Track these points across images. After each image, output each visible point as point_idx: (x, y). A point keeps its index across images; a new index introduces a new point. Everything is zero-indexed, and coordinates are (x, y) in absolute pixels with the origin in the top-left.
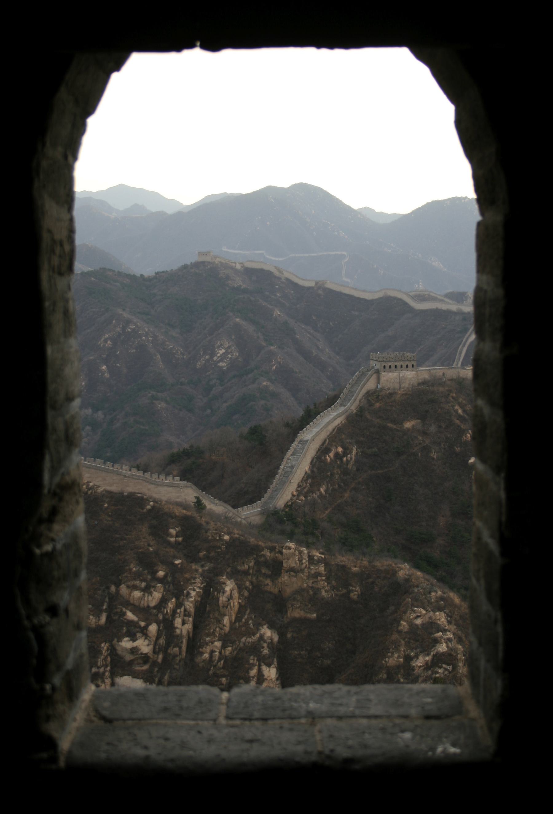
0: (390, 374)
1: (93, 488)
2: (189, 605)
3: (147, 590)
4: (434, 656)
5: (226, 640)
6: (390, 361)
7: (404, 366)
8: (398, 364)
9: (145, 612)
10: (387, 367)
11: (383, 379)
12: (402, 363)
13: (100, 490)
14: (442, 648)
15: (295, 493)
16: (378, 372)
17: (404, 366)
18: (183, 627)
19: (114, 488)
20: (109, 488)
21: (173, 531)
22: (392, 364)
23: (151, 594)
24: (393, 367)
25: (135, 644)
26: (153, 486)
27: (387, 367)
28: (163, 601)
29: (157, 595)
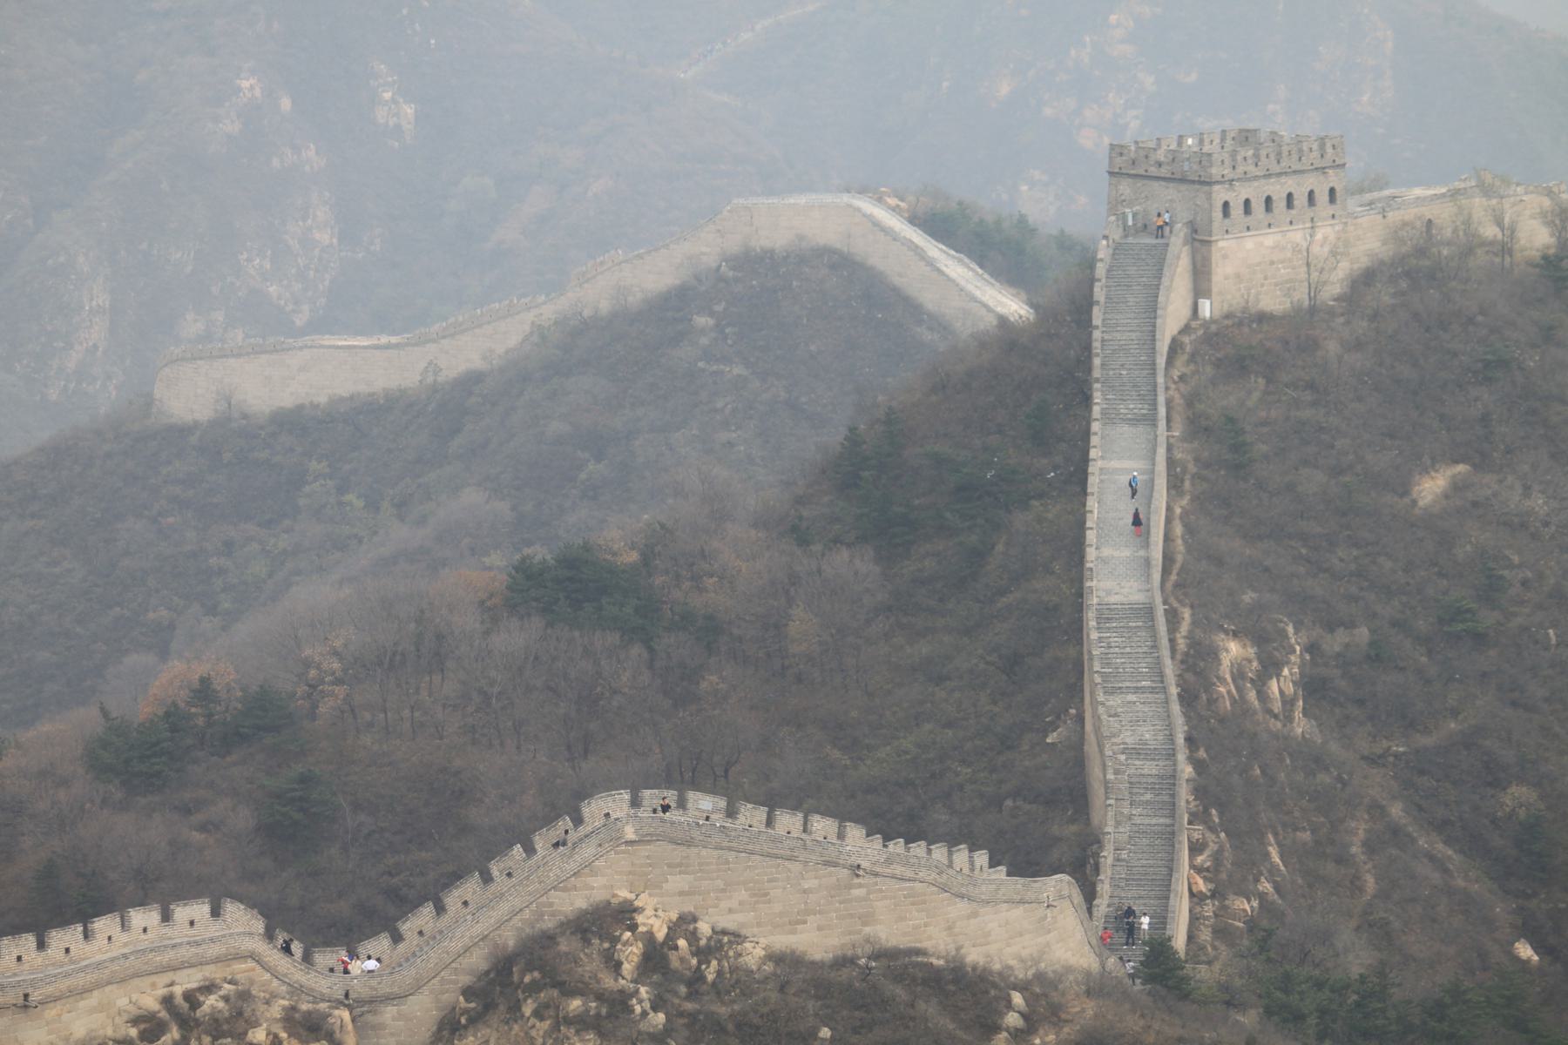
0: (1249, 244)
1: (720, 947)
6: (1246, 178)
7: (1300, 200)
8: (1278, 189)
10: (1237, 210)
11: (1223, 271)
12: (1290, 184)
13: (753, 955)
15: (1201, 885)
16: (1199, 240)
17: (1300, 200)
19: (817, 941)
20: (782, 941)
22: (1254, 192)
26: (962, 907)
27: (1237, 210)
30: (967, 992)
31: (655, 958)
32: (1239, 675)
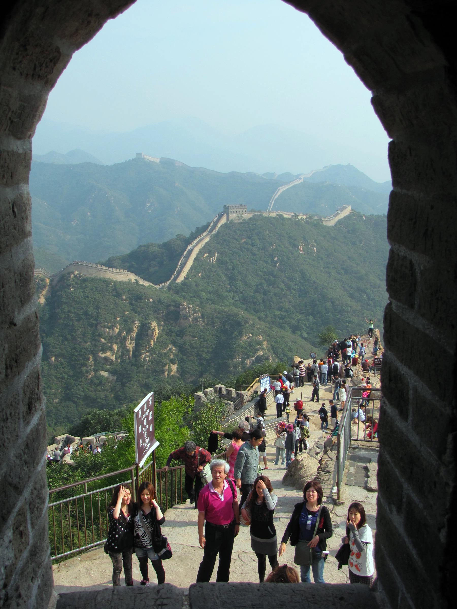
2: (134, 335)
3: (112, 328)
4: (256, 358)
5: (152, 351)
8: (238, 210)
9: (111, 339)
14: (260, 353)
18: (130, 346)
21: (124, 298)
23: (113, 329)
24: (235, 212)
25: (106, 355)
27: (232, 212)
28: (120, 333)
29: (117, 330)
30: (106, 282)
31: (75, 276)
32: (207, 257)
